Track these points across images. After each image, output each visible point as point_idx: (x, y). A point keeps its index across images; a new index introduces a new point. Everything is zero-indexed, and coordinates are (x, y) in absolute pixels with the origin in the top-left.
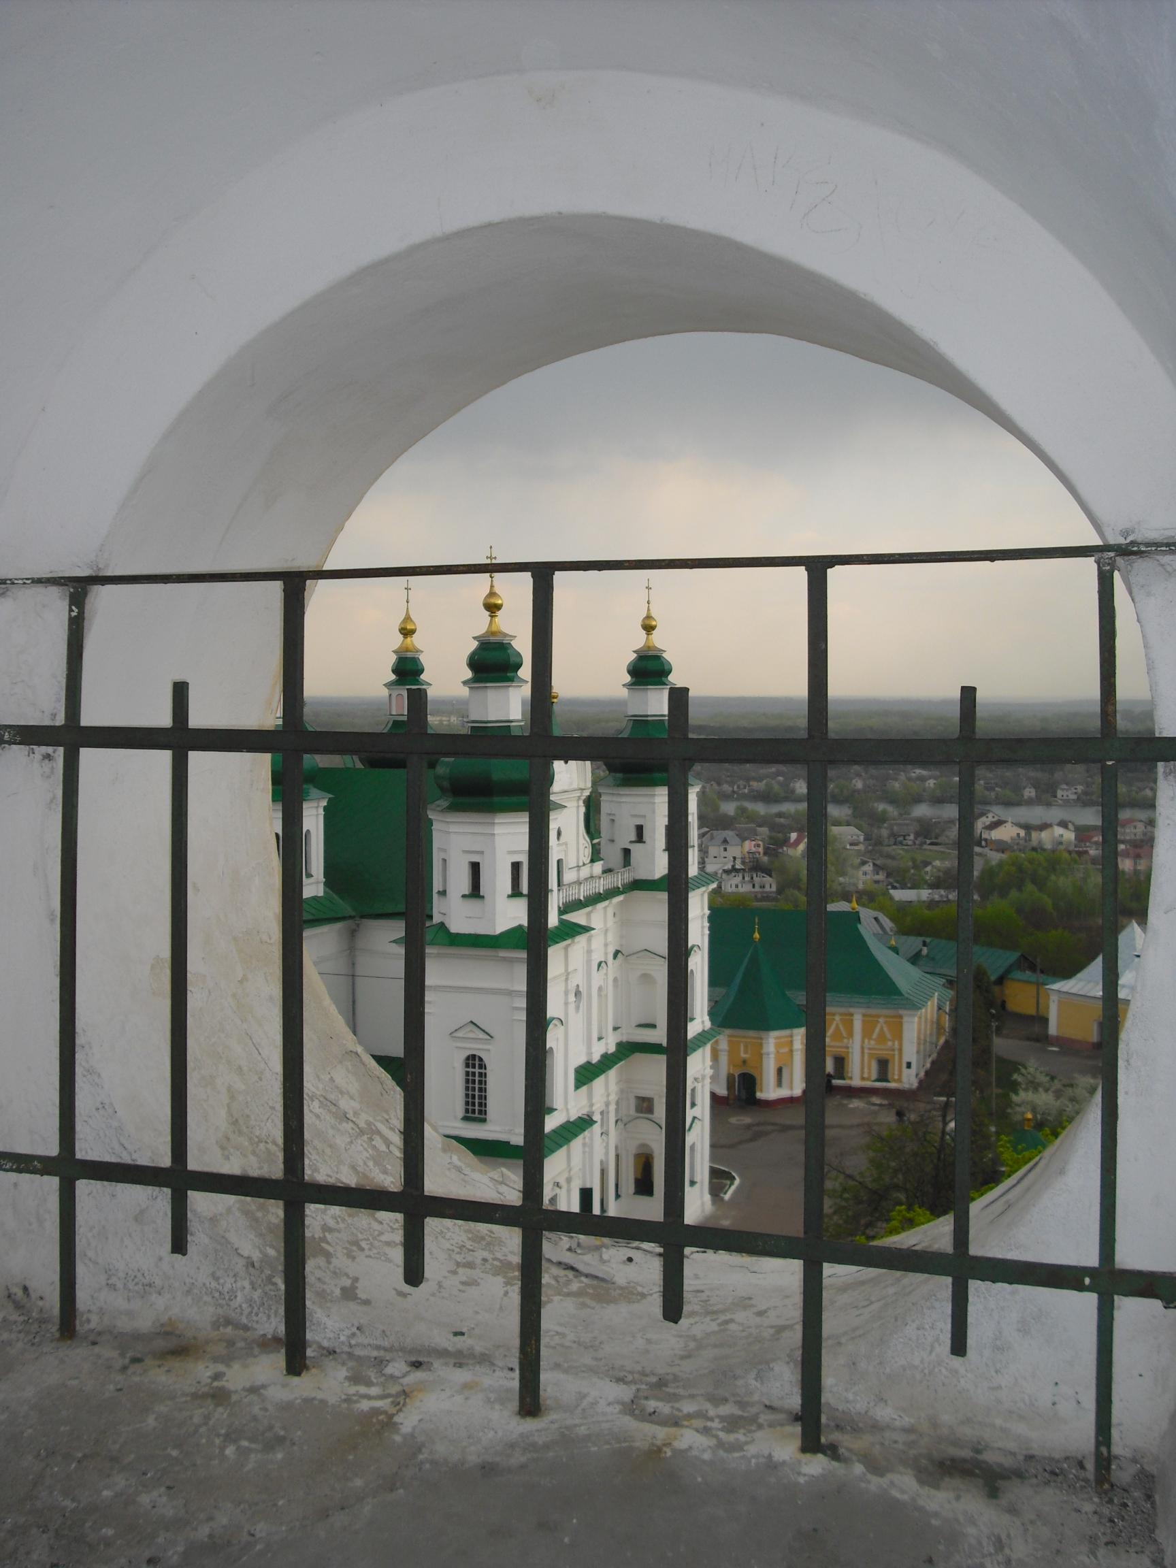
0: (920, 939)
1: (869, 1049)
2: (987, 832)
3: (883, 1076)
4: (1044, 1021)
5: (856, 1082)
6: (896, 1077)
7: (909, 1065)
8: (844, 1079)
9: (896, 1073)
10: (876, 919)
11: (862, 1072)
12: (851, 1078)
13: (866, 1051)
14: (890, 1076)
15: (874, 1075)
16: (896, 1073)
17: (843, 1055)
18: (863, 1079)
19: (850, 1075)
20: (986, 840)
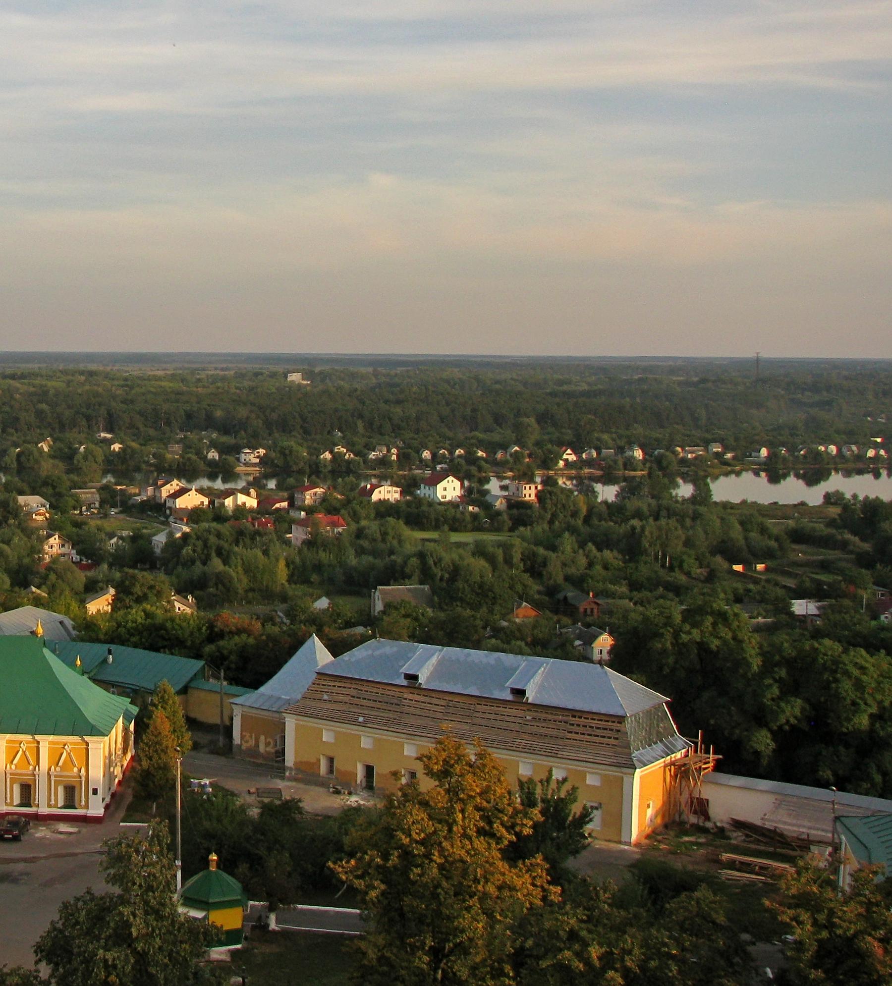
0: (106, 647)
1: (55, 776)
2: (171, 500)
3: (70, 803)
4: (228, 731)
5: (44, 810)
6: (83, 803)
7: (95, 792)
8: (31, 806)
9: (83, 798)
10: (61, 623)
11: (49, 800)
12: (38, 806)
13: (53, 778)
14: (77, 806)
15: (61, 803)
16: (83, 798)
17: (30, 782)
18: (49, 806)
19: (37, 802)
20: (170, 508)
